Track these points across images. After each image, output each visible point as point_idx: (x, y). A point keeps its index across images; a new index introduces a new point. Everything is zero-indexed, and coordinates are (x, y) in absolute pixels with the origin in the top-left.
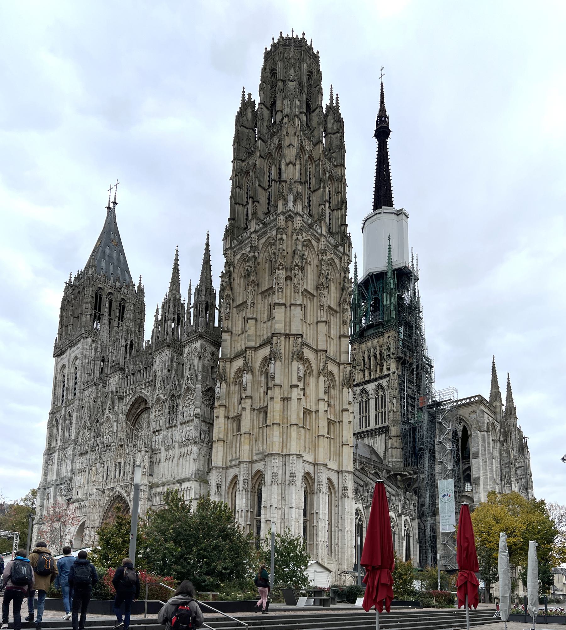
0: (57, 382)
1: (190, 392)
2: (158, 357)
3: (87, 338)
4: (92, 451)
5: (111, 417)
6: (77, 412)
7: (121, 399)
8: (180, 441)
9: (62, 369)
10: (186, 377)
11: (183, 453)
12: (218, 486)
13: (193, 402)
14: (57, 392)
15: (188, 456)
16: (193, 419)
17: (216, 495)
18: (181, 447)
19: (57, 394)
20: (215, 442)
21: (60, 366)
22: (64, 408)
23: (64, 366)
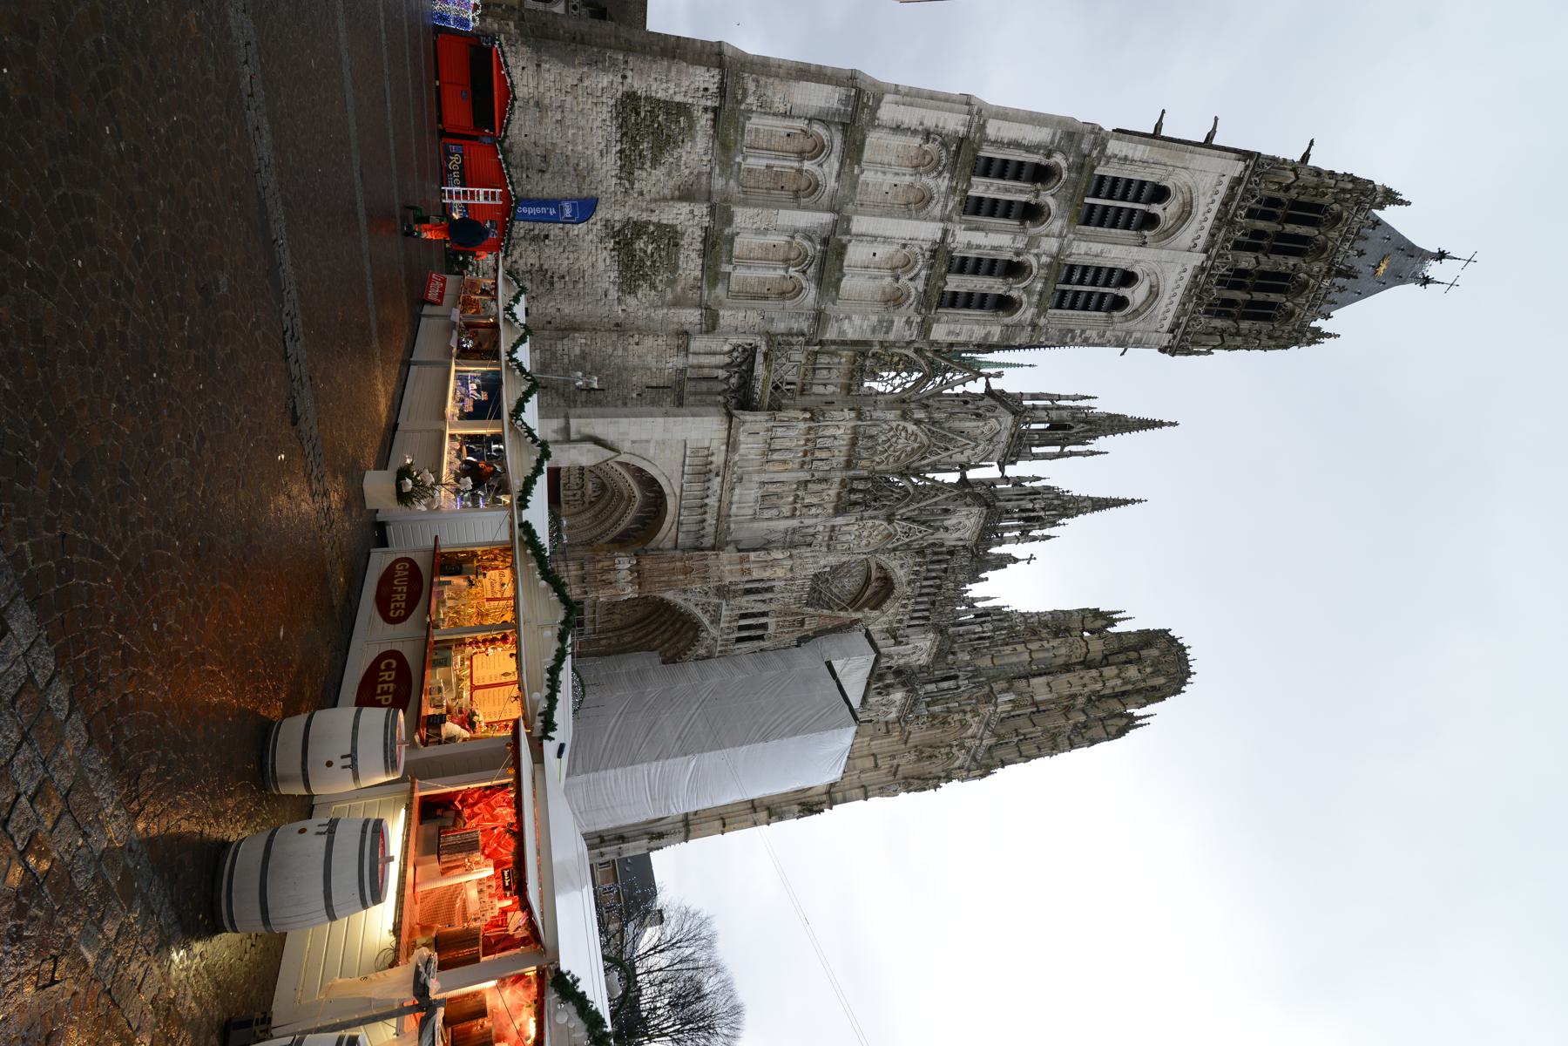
0: (1171, 169)
2: (928, 643)
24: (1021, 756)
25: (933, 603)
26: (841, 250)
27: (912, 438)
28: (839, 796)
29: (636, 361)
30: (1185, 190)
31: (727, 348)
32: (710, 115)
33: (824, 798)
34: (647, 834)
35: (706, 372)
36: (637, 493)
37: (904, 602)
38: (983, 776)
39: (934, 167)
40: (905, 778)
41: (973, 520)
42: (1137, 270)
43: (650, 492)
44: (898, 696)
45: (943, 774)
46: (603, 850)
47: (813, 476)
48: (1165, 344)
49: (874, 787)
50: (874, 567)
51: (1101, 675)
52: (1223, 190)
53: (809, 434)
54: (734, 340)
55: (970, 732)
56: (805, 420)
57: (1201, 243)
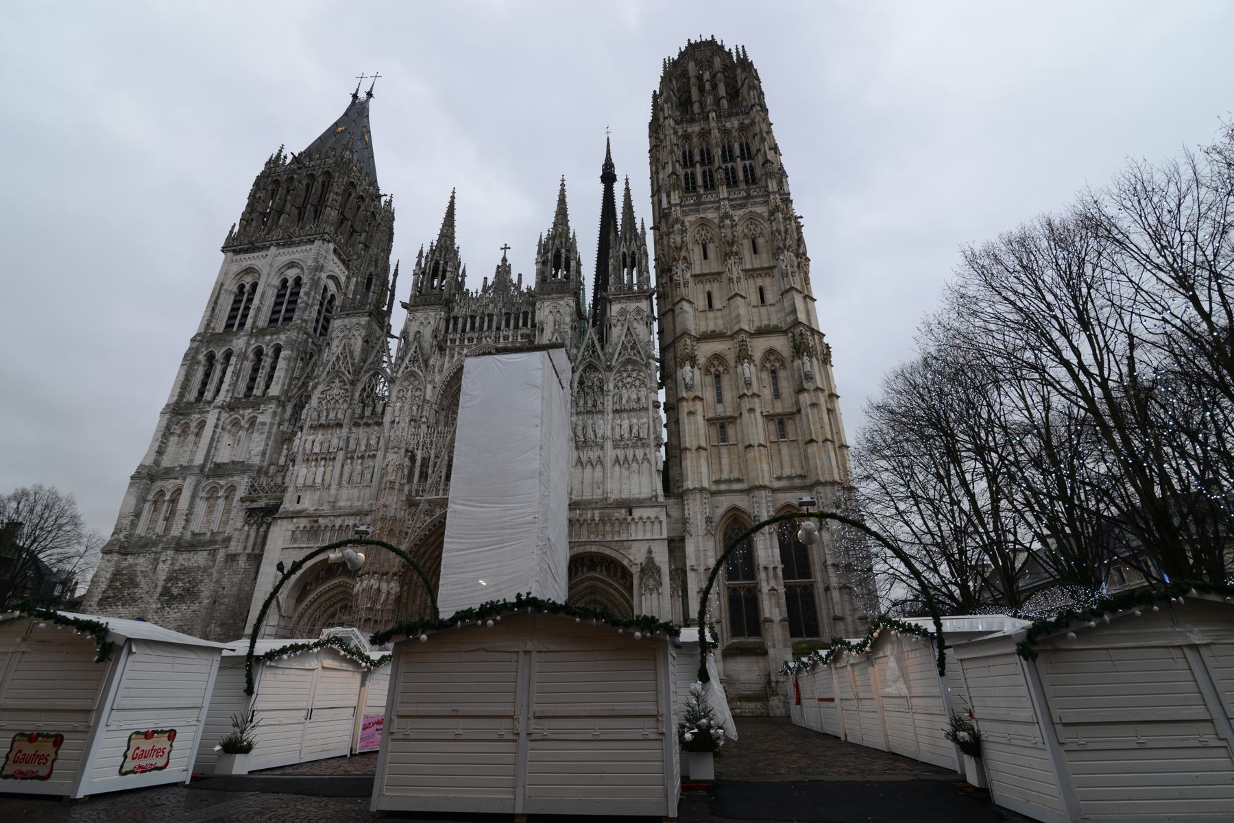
0: (222, 292)
1: (630, 367)
2: (546, 304)
3: (329, 242)
4: (357, 425)
5: (421, 374)
6: (292, 351)
8: (618, 438)
9: (241, 275)
11: (621, 458)
12: (709, 520)
13: (637, 383)
14: (218, 307)
16: (647, 409)
17: (709, 535)
18: (615, 447)
19: (217, 310)
20: (690, 450)
21: (235, 268)
22: (245, 338)
23: (250, 270)
26: (218, 466)
27: (333, 385)
28: (790, 319)
29: (235, 588)
30: (238, 277)
31: (246, 528)
32: (129, 557)
33: (790, 335)
35: (259, 540)
36: (336, 581)
39: (187, 425)
41: (418, 315)
42: (276, 282)
43: (338, 570)
47: (341, 449)
48: (321, 242)
49: (782, 285)
52: (238, 257)
53: (308, 460)
54: (239, 525)
55: (710, 215)
56: (293, 466)
57: (264, 253)
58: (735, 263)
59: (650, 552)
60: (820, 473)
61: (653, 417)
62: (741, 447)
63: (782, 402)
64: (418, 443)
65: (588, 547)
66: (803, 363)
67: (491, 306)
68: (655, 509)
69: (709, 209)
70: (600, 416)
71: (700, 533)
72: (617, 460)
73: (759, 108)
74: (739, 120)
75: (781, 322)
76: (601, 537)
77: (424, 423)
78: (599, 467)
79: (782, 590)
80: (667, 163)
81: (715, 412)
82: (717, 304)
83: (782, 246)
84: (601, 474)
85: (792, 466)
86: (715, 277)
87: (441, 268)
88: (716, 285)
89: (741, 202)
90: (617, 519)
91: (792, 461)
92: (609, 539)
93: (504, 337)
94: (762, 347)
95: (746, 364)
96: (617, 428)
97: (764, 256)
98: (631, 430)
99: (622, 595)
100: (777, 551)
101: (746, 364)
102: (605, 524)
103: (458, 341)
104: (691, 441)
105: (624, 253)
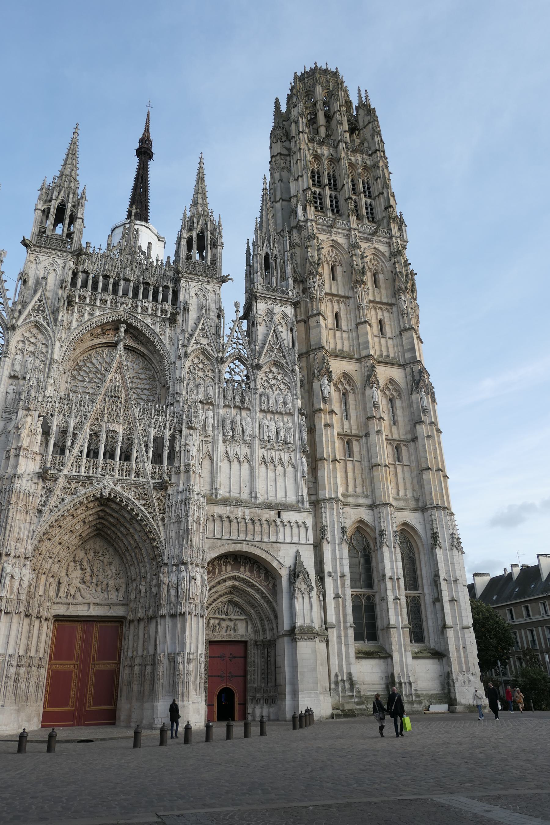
1: (274, 370)
2: (192, 284)
7: (70, 303)
8: (266, 438)
10: (268, 343)
15: (280, 468)
18: (262, 447)
24: (382, 193)
25: (147, 284)
28: (408, 355)
33: (408, 369)
34: (432, 549)
37: (139, 310)
38: (401, 223)
40: (394, 295)
41: (42, 258)
44: (261, 307)
45: (393, 261)
46: (446, 598)
49: (401, 323)
50: (102, 340)
51: (294, 137)
55: (341, 240)
58: (364, 291)
59: (297, 555)
60: (434, 498)
61: (299, 424)
62: (366, 464)
63: (398, 427)
64: (53, 408)
65: (239, 545)
66: (421, 398)
67: (128, 271)
68: (302, 514)
69: (339, 233)
70: (248, 412)
71: (337, 542)
72: (264, 461)
73: (382, 155)
74: (363, 159)
75: (398, 356)
76: (251, 537)
77: (51, 385)
78: (245, 465)
79: (403, 599)
80: (302, 176)
81: (343, 428)
82: (344, 325)
83: (403, 287)
84: (248, 472)
85: (405, 489)
86: (343, 299)
87: (68, 212)
88: (343, 307)
89: (368, 236)
90: (267, 520)
91: (405, 483)
92: (258, 538)
93: (142, 308)
94: (384, 376)
95: (375, 389)
96: (266, 430)
97: (383, 292)
98: (277, 433)
99: (265, 597)
100: (400, 564)
101: (375, 389)
102: (254, 525)
103: (88, 299)
104: (328, 452)
105: (267, 255)
